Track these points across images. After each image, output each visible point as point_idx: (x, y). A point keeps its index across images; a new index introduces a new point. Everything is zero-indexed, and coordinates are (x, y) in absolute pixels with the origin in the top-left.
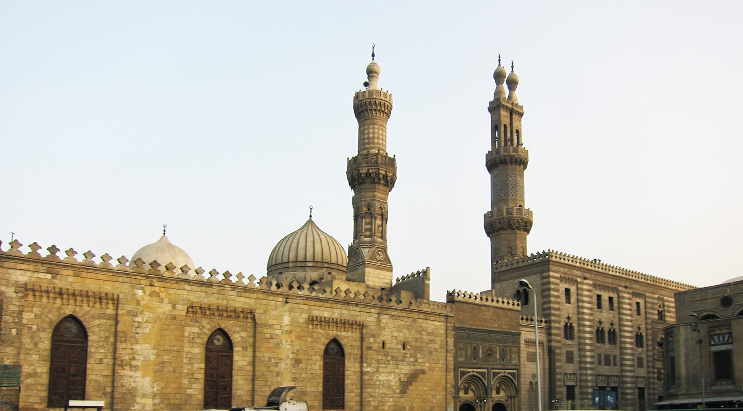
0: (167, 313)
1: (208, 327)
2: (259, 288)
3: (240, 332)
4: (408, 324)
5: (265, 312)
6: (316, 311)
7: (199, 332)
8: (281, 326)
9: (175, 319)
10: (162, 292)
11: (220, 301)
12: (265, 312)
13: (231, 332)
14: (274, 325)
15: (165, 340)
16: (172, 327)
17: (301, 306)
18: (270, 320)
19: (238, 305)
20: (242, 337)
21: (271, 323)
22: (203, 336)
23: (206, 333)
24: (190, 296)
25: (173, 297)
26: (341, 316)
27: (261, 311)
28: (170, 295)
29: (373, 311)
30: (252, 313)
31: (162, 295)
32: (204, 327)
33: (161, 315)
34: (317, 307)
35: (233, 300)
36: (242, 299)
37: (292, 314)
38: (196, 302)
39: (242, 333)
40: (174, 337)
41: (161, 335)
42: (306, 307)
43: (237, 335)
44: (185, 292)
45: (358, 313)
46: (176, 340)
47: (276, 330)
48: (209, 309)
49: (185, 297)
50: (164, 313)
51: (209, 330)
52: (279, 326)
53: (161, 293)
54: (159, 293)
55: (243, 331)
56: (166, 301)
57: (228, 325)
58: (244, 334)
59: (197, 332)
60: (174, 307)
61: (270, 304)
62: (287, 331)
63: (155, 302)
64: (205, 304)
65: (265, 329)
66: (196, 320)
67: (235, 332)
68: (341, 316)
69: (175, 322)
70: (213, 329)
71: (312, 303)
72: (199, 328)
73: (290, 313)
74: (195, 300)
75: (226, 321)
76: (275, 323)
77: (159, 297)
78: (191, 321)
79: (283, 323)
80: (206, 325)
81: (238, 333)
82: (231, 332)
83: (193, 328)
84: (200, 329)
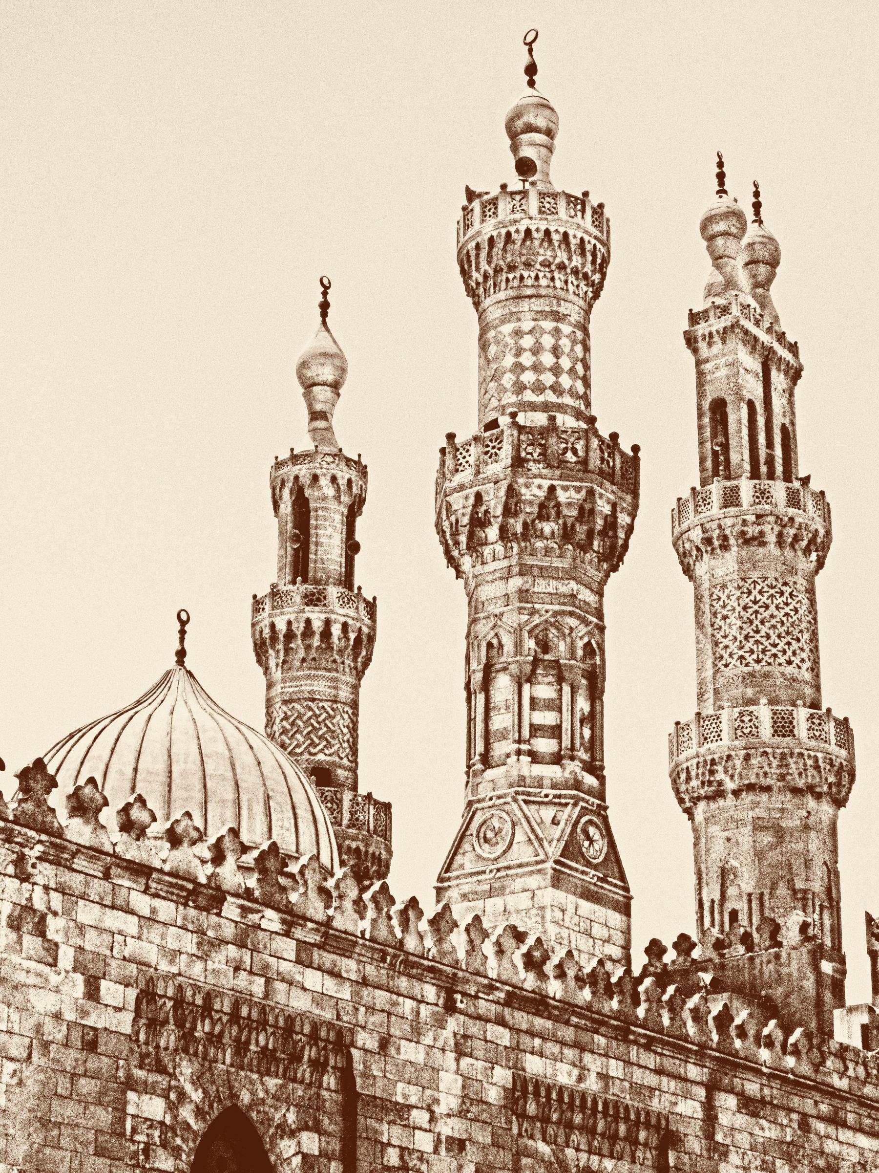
0: (70, 1015)
1: (197, 1096)
2: (367, 936)
3: (299, 1130)
4: (789, 1139)
5: (384, 1043)
6: (536, 1058)
7: (168, 1120)
8: (433, 1119)
9: (91, 1046)
10: (55, 914)
11: (242, 981)
12: (384, 1043)
13: (272, 1130)
14: (411, 1107)
15: (59, 1148)
16: (86, 1086)
17: (494, 1031)
18: (400, 1086)
19: (300, 1003)
20: (305, 1156)
21: (400, 1100)
22: (178, 1141)
23: (188, 1125)
24: (145, 944)
25: (92, 942)
26: (606, 1088)
27: (372, 1044)
28: (81, 929)
29: (693, 1072)
30: (342, 1042)
31: (55, 927)
32: (182, 1096)
33: (49, 1026)
34: (537, 1042)
35: (283, 980)
36: (313, 979)
37: (465, 1062)
38: (169, 977)
39: (305, 1136)
40: (91, 1135)
41: (45, 1123)
42: (504, 1037)
43: (287, 1147)
44: (130, 924)
45: (651, 1080)
46: (95, 1155)
47: (417, 1131)
48: (207, 1009)
49: (132, 948)
50: (58, 1016)
51: (199, 1112)
52: (427, 1116)
53: (50, 918)
54: (43, 918)
55: (307, 1128)
56: (66, 957)
57: (261, 1095)
58: (311, 1142)
59: (159, 1118)
60: (92, 993)
61: (400, 1009)
62: (450, 1140)
63: (30, 959)
64: (196, 988)
65: (385, 1126)
66: (158, 1060)
67: (285, 1131)
68: (606, 1088)
69: (93, 1063)
70: (211, 1106)
71: (521, 1019)
72: (167, 1097)
73: (457, 1060)
74: (164, 967)
75: (255, 1076)
76: (413, 1100)
77: (42, 934)
78: (141, 1067)
79: (437, 1101)
80: (188, 1088)
81: (292, 1134)
82: (272, 1130)
83: (146, 1097)
84: (172, 1107)
